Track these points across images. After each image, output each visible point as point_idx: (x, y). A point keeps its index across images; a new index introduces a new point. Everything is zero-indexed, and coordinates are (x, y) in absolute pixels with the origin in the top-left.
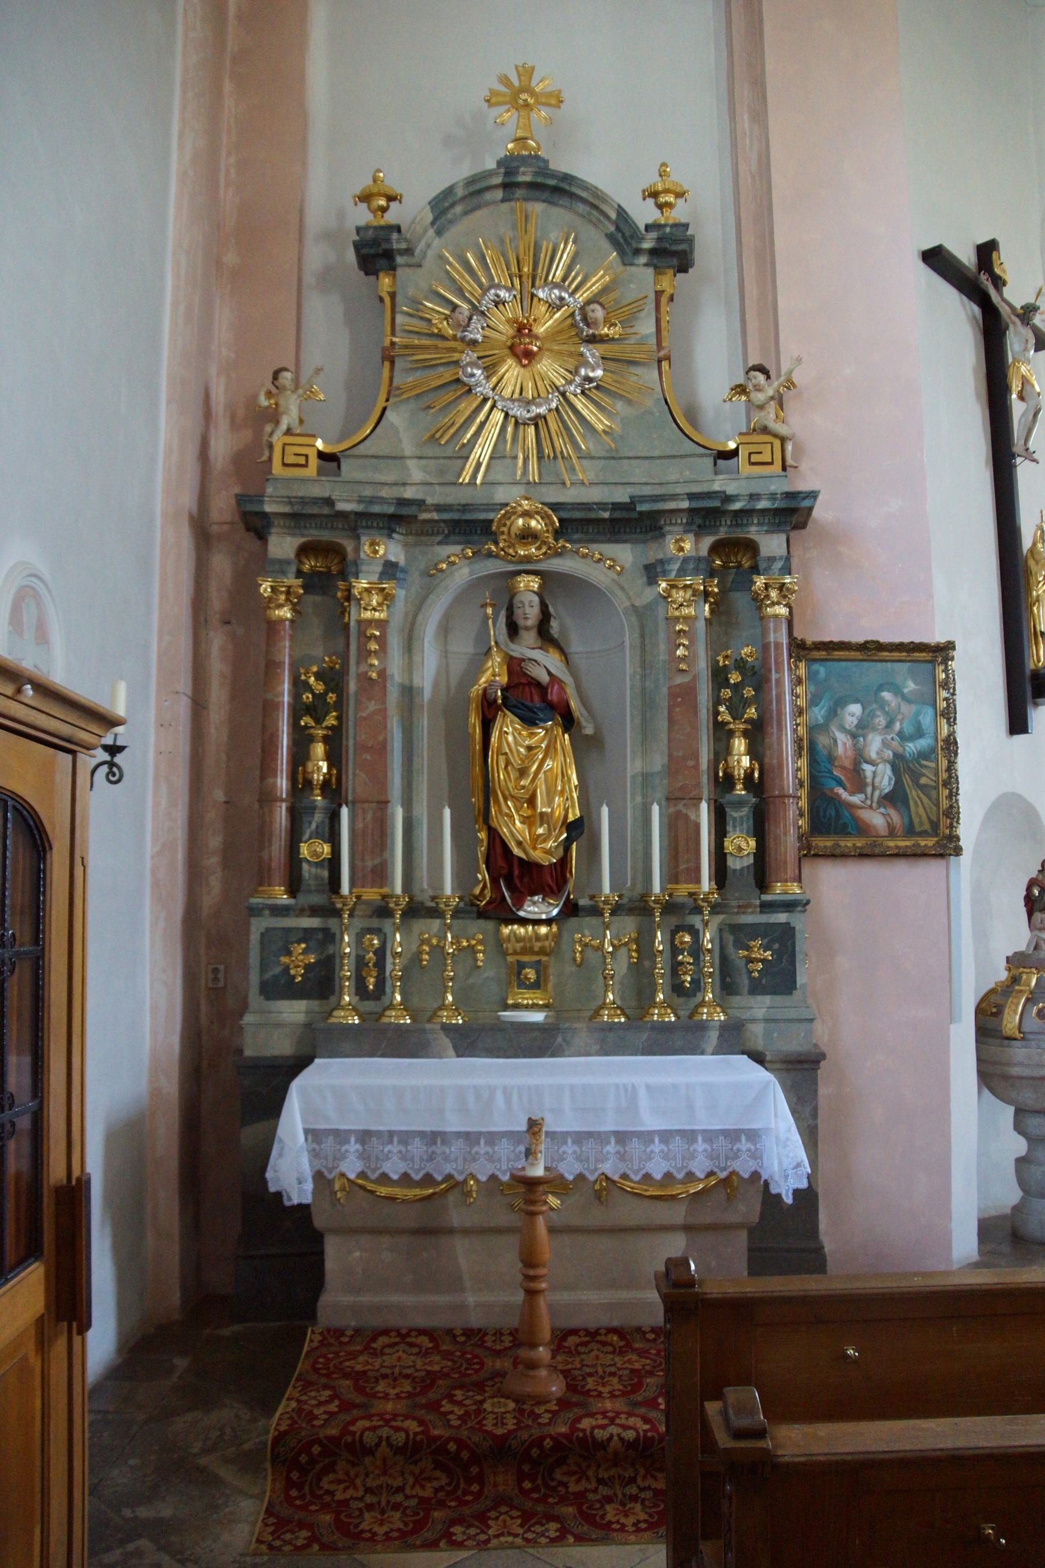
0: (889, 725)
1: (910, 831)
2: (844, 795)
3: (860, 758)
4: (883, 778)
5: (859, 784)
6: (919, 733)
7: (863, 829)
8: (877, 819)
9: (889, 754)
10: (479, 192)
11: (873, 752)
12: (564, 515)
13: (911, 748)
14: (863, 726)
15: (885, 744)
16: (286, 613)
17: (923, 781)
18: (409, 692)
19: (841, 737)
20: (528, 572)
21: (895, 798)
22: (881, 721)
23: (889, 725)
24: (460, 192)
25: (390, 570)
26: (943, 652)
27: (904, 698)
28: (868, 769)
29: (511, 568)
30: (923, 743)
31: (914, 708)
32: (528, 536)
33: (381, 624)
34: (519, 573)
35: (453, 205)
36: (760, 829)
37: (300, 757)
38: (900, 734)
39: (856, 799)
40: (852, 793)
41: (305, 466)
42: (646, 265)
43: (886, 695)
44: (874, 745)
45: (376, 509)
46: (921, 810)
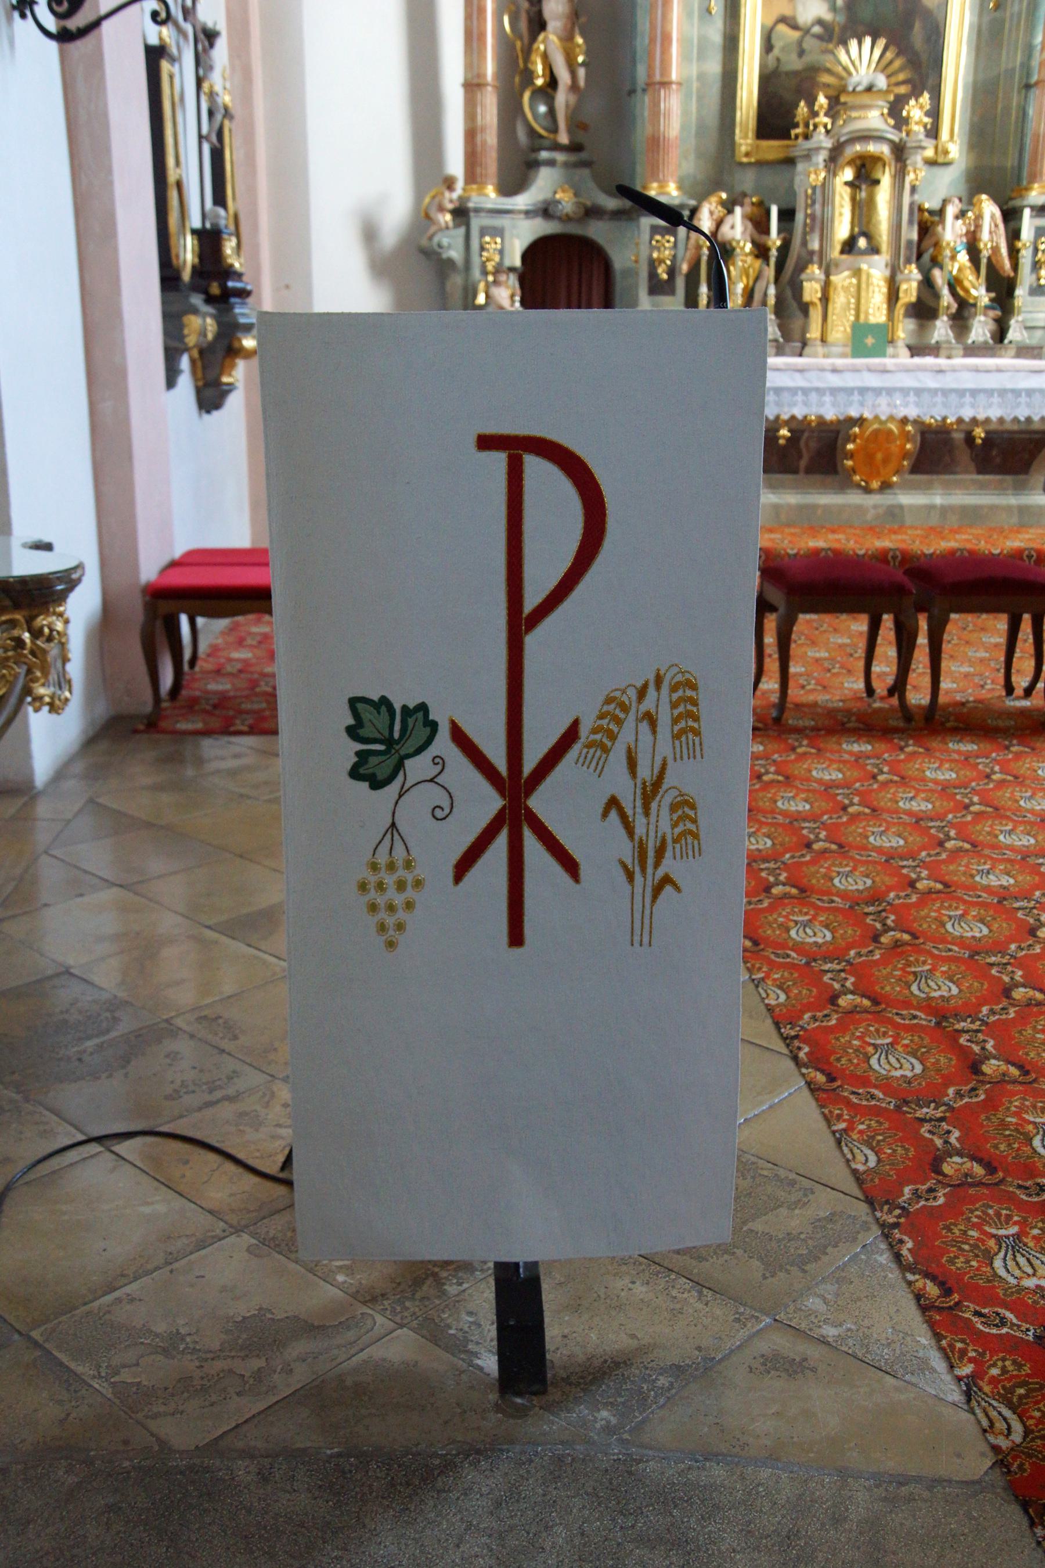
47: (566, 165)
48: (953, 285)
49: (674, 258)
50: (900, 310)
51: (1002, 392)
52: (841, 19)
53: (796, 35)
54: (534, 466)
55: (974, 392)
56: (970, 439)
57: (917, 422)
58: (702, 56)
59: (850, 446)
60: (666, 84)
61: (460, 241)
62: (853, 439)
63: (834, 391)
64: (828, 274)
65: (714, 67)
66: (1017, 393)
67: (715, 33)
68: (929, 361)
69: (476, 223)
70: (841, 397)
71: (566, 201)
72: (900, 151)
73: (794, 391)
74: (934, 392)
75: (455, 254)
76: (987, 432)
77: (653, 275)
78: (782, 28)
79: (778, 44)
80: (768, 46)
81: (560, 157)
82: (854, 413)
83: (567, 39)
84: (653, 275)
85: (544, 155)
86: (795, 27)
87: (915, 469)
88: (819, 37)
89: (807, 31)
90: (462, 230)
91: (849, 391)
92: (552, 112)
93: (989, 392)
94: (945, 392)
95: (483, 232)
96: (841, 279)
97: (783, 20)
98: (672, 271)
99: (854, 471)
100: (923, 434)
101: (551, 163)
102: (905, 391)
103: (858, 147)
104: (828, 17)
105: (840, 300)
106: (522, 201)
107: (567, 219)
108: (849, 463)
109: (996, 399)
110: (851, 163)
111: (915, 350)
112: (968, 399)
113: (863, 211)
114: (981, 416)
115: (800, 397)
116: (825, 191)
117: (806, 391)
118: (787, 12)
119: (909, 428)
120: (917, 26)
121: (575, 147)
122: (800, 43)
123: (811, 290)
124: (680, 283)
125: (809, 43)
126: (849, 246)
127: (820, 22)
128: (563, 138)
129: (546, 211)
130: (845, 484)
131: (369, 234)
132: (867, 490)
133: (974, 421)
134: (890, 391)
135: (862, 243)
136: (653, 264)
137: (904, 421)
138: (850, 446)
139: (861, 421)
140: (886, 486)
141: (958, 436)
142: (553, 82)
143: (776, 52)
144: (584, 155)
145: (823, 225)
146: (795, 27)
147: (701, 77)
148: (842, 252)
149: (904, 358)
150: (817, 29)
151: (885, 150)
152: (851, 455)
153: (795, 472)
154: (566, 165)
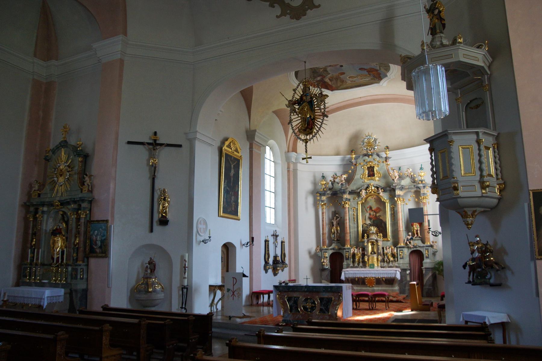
0: (100, 235)
1: (102, 253)
2: (94, 246)
3: (96, 240)
4: (99, 243)
5: (96, 245)
6: (104, 236)
7: (96, 252)
8: (98, 251)
9: (100, 239)
10: (58, 148)
11: (98, 239)
12: (61, 202)
13: (103, 238)
14: (97, 235)
15: (100, 238)
16: (31, 219)
17: (104, 244)
18: (46, 230)
19: (94, 236)
20: (60, 211)
21: (100, 247)
22: (99, 233)
23: (100, 235)
24: (55, 148)
25: (43, 212)
26: (107, 221)
27: (102, 229)
28: (97, 242)
29: (58, 210)
30: (105, 237)
31: (104, 231)
32: (58, 205)
33: (41, 221)
34: (59, 211)
35: (55, 150)
36: (77, 254)
37: (32, 241)
38: (102, 236)
39: (95, 247)
40: (95, 246)
41: (36, 196)
42: (77, 157)
43: (100, 229)
44: (98, 238)
45: (38, 203)
46: (104, 249)
47: (336, 243)
48: (388, 258)
49: (349, 255)
50: (379, 262)
51: (386, 273)
52: (372, 223)
53: (366, 225)
54: (234, 279)
55: (382, 273)
56: (383, 280)
57: (375, 277)
58: (354, 228)
59: (366, 281)
60: (347, 233)
61: (321, 254)
62: (366, 280)
63: (363, 273)
64: (368, 257)
65: (356, 230)
66: (389, 273)
67: (356, 226)
68: (382, 269)
69: (323, 251)
70: (384, 274)
71: (337, 247)
72: (377, 241)
73: (357, 273)
74: (377, 273)
75: (320, 255)
76: (385, 279)
77: (346, 257)
78: (364, 225)
79: (364, 227)
80: (363, 227)
81: (335, 242)
82: (366, 276)
83: (337, 227)
84: (346, 257)
85: (333, 242)
86: (366, 224)
87: (377, 284)
88: (369, 226)
89: (368, 225)
90: (321, 252)
91: (365, 273)
92: (334, 236)
93: (385, 273)
94: (378, 273)
95: (324, 252)
96: (370, 258)
97: (364, 224)
98: (348, 257)
99: (367, 284)
100: (376, 279)
101: (334, 243)
102: (373, 273)
103: (370, 240)
104: (371, 223)
105: (370, 260)
106: (330, 248)
107: (337, 250)
108: (367, 283)
109: (385, 274)
110: (371, 242)
111: (381, 267)
112: (382, 274)
113: (373, 248)
114: (384, 276)
115: (358, 274)
116: (368, 247)
117: (359, 273)
118: (365, 223)
119: (374, 278)
120: (383, 224)
121: (337, 240)
122: (367, 226)
123: (366, 259)
124: (350, 259)
125: (368, 226)
126: (371, 253)
127: (369, 224)
128: (336, 240)
129: (333, 249)
130: (367, 286)
131: (310, 253)
132: (370, 287)
133: (383, 277)
134: (371, 273)
135: (373, 253)
136: (346, 256)
137: (373, 277)
138: (366, 281)
139: (367, 277)
140: (372, 287)
141: (381, 279)
142: (334, 233)
143: (364, 228)
144: (339, 242)
145: (368, 251)
146: (366, 224)
147: (354, 231)
148: (371, 254)
149: (380, 269)
150: (369, 225)
151: (374, 241)
152: (367, 282)
153: (360, 284)
154: (336, 243)
